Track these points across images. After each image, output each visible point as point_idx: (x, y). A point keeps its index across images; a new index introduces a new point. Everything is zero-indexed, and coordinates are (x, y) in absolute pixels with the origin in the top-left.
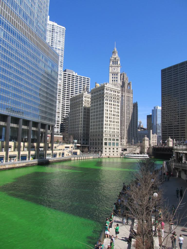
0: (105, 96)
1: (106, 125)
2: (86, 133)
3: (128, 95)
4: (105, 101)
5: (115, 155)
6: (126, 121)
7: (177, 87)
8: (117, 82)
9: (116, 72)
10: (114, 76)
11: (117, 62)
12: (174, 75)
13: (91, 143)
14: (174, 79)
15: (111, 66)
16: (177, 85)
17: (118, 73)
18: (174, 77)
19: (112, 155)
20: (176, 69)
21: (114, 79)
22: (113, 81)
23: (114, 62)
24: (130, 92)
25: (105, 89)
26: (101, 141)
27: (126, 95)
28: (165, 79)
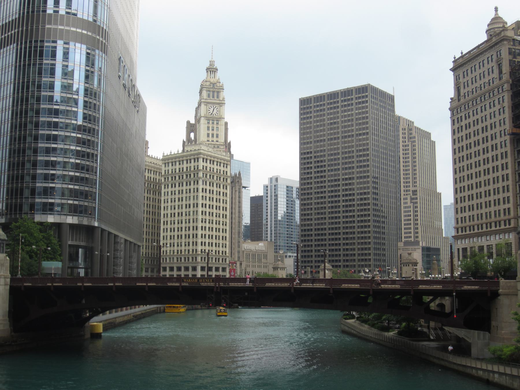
4: (201, 187)
8: (217, 139)
15: (204, 102)
16: (335, 139)
20: (335, 103)
22: (208, 135)
28: (308, 123)
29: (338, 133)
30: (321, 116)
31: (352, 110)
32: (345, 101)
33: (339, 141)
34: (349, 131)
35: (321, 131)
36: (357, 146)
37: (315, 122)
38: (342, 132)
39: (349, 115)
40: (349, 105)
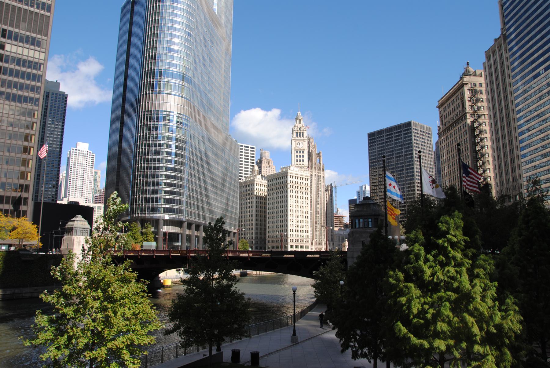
0: (289, 186)
3: (317, 174)
6: (314, 216)
10: (299, 154)
11: (303, 133)
12: (386, 142)
14: (387, 149)
18: (386, 146)
20: (390, 134)
21: (299, 159)
22: (297, 161)
24: (320, 168)
25: (289, 177)
27: (314, 174)
28: (373, 149)
29: (393, 154)
30: (382, 143)
32: (397, 133)
34: (400, 153)
37: (378, 148)
38: (396, 154)
39: (399, 142)
40: (399, 136)
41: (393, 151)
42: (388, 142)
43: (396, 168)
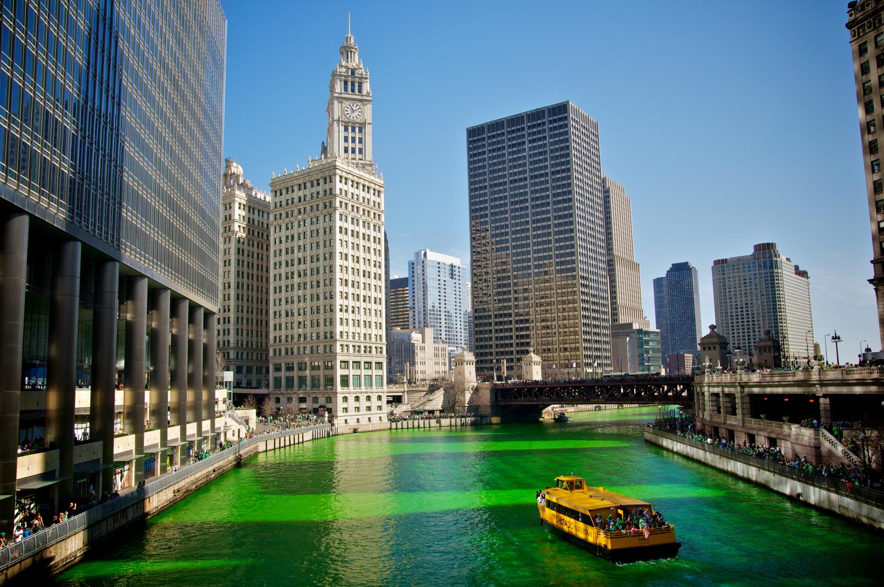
1: (350, 312)
2: (244, 346)
4: (338, 223)
5: (375, 419)
7: (521, 187)
9: (358, 121)
11: (360, 86)
13: (278, 381)
14: (510, 161)
15: (338, 97)
17: (365, 124)
18: (510, 154)
19: (364, 421)
20: (518, 130)
21: (350, 145)
22: (346, 151)
23: (349, 84)
26: (327, 372)
29: (525, 172)
30: (499, 149)
31: (545, 138)
33: (527, 182)
35: (500, 170)
36: (554, 188)
38: (531, 170)
39: (540, 147)
41: (525, 164)
42: (514, 145)
43: (533, 199)
